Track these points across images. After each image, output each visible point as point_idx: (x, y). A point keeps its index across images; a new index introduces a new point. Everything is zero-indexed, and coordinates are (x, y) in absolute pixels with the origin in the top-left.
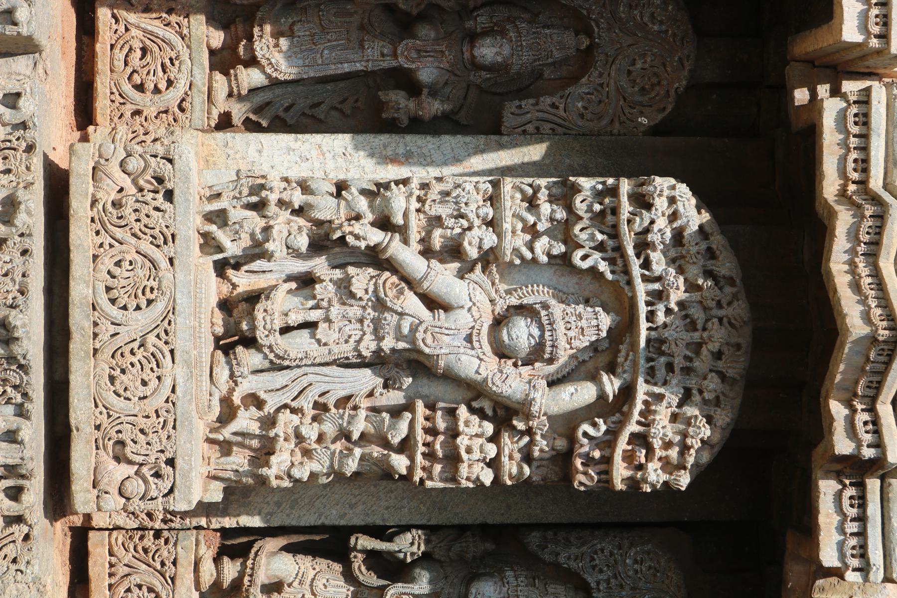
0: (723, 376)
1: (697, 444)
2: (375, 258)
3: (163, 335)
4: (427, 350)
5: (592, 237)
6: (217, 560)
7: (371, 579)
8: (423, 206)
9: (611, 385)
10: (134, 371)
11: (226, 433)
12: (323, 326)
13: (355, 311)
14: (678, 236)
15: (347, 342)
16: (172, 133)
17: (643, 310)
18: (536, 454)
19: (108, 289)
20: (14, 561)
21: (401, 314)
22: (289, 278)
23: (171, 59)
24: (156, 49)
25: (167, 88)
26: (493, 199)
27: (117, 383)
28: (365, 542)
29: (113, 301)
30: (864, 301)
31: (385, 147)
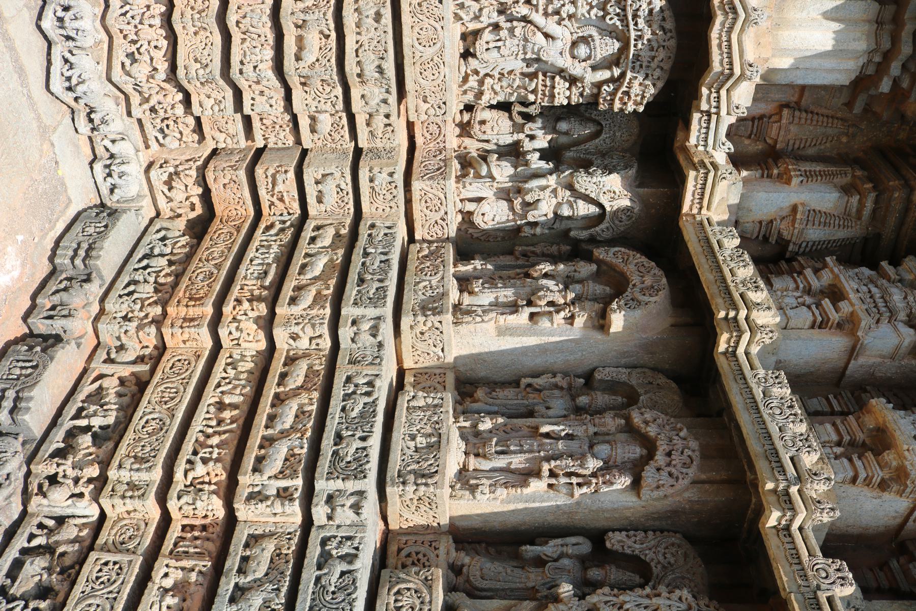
0: (662, 69)
1: (647, 95)
2: (525, 19)
5: (615, 10)
6: (461, 112)
9: (617, 72)
11: (465, 88)
12: (503, 48)
13: (516, 41)
14: (651, 11)
17: (633, 42)
18: (585, 94)
22: (489, 25)
28: (518, 108)
30: (721, 54)
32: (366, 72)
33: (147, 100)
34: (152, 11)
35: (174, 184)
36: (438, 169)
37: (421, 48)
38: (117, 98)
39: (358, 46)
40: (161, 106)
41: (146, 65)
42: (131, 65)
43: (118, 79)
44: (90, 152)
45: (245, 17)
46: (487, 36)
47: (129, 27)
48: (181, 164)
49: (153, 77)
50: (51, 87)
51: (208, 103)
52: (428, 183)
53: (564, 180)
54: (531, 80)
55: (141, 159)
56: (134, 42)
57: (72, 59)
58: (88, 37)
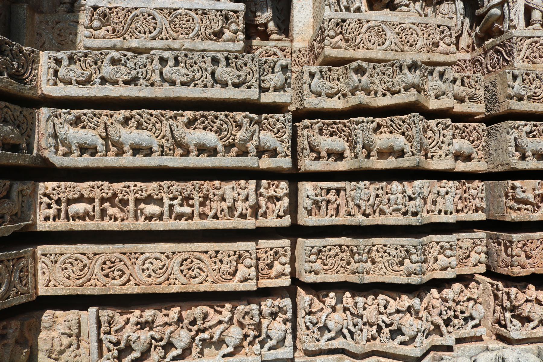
10: (408, 37)
16: (295, 51)
19: (379, 45)
20: (476, 82)
23: (266, 53)
25: (277, 55)
27: (413, 44)
29: (383, 44)
32: (416, 81)
33: (437, 327)
35: (525, 314)
36: (498, 52)
37: (387, 43)
39: (388, 94)
40: (444, 313)
41: (404, 319)
42: (403, 334)
43: (418, 349)
45: (359, 206)
48: (501, 305)
49: (417, 312)
51: (443, 260)
52: (515, 54)
56: (379, 328)
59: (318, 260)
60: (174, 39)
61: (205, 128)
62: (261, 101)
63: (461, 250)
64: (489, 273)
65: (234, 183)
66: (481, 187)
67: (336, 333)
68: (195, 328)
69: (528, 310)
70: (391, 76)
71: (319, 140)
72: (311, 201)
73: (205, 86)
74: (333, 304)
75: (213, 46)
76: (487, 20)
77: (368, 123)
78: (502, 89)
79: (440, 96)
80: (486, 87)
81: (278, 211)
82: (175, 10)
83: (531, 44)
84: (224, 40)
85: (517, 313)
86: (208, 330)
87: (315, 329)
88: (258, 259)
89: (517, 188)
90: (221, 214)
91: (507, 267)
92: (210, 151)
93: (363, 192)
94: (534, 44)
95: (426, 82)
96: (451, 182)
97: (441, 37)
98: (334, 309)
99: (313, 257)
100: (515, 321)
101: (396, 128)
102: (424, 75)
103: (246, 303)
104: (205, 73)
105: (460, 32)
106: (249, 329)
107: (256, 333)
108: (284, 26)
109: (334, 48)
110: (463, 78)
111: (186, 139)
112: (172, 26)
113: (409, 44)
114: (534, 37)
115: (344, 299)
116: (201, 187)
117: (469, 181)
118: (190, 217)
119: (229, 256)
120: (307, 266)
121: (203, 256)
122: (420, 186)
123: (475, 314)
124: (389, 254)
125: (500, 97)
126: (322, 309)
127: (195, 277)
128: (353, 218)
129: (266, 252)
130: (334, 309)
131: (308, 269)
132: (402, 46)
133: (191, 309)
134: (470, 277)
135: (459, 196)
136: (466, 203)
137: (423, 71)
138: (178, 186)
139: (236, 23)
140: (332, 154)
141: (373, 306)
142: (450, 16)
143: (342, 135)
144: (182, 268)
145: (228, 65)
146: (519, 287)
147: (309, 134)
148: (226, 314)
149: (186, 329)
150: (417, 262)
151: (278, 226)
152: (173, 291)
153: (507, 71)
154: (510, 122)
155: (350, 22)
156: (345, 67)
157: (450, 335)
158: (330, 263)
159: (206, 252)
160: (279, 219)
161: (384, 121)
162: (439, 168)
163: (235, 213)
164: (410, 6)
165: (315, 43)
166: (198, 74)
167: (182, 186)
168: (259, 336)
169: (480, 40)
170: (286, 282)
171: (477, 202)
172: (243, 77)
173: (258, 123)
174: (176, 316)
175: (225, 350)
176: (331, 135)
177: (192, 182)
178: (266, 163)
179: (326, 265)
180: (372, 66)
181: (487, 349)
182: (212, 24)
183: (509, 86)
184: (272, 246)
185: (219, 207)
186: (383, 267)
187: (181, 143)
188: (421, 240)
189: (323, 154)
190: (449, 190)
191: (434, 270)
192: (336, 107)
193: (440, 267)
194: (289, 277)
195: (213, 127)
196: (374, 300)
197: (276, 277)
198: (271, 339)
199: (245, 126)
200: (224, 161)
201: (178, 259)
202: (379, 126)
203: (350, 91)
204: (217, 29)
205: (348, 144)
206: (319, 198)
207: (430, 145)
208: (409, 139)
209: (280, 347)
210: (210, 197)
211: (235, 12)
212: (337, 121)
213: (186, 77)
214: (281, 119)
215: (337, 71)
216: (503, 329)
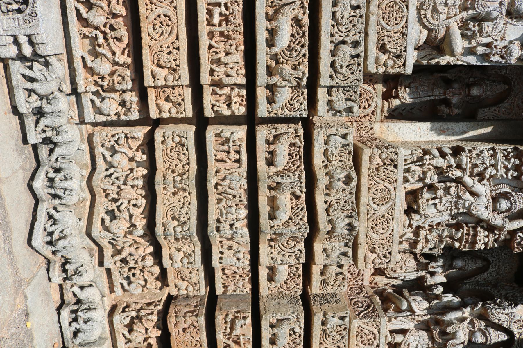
2: (459, 181)
3: (390, 213)
4: (474, 213)
7: (423, 260)
8: (471, 160)
10: (380, 225)
12: (438, 204)
13: (450, 199)
15: (447, 210)
16: (372, 124)
19: (373, 199)
20: (339, 286)
21: (465, 200)
24: (365, 94)
26: (494, 156)
27: (374, 229)
29: (374, 203)
31: (441, 126)
32: (338, 230)
33: (119, 252)
34: (135, 174)
35: (135, 327)
36: (368, 306)
37: (375, 206)
38: (91, 250)
39: (327, 206)
40: (132, 258)
41: (124, 222)
42: (111, 221)
43: (98, 234)
44: (57, 297)
45: (224, 179)
46: (427, 195)
47: (113, 187)
48: (142, 309)
49: (131, 233)
50: (33, 242)
52: (365, 321)
53: (477, 312)
54: (457, 230)
55: (106, 304)
56: (115, 201)
57: (56, 215)
58: (74, 196)
59: (175, 144)
60: (379, 6)
61: (293, 35)
62: (319, 88)
63: (189, 272)
64: (170, 298)
65: (242, 63)
66: (245, 290)
67: (110, 162)
68: (108, 30)
69: (138, 329)
70: (343, 208)
71: (285, 143)
72: (228, 136)
73: (332, 35)
74: (136, 158)
75: (372, 44)
76: (398, 298)
77: (300, 189)
78: (332, 308)
79: (326, 253)
80: (336, 295)
81: (218, 105)
82: (407, 6)
83: (373, 334)
84: (377, 54)
85: (135, 321)
86: (106, 42)
87: (112, 143)
88: (173, 87)
89: (245, 320)
90: (213, 52)
91: (176, 313)
92: (271, 40)
93: (237, 183)
94: (374, 336)
95: (338, 240)
96: (248, 263)
97: (381, 255)
98: (131, 160)
99: (177, 139)
100: (128, 320)
101: (296, 212)
102: (344, 238)
103: (133, 77)
104: (344, 35)
105: (389, 276)
106: (109, 81)
107: (106, 87)
108: (397, 115)
109: (371, 157)
110: (343, 274)
111: (282, 17)
112: (391, 4)
113: (374, 226)
114: (380, 336)
115: (141, 168)
116: (238, 33)
117: (250, 280)
118: (210, 23)
119: (175, 60)
120: (169, 134)
121: (173, 36)
122: (243, 234)
123: (133, 286)
124: (182, 208)
125: (325, 307)
126: (131, 149)
127: (154, 29)
128: (213, 175)
129: (180, 95)
130: (131, 160)
131: (166, 135)
132: (372, 219)
133: (125, 25)
134: (166, 283)
135: (237, 271)
136: (231, 277)
137: (348, 237)
138: (238, 11)
139: (394, 65)
140: (272, 155)
141: (135, 195)
142: (403, 267)
143: (290, 164)
144: (162, 16)
145: (353, 57)
146: (158, 323)
147: (290, 134)
148: (122, 59)
149: (106, 21)
150: (175, 232)
151: (204, 105)
152: (140, 8)
153: (349, 312)
154: (303, 314)
155: (394, 172)
156: (352, 167)
157: (113, 263)
158: (172, 154)
159: (177, 39)
160: (211, 106)
161: (302, 202)
162: (261, 252)
163: (215, 65)
164: (410, 228)
165: (377, 142)
166: (343, 28)
167: (238, 14)
168: (104, 91)
169: (381, 293)
170: (154, 114)
171: (231, 287)
172: (340, 71)
173: (299, 85)
174: (117, 12)
175: (89, 59)
176: (290, 155)
177: (242, 24)
178: (262, 94)
179: (171, 151)
180: (352, 191)
181: (103, 296)
182: (393, 43)
183: (334, 313)
184: (186, 100)
185: (219, 50)
186: (170, 202)
187: (278, 13)
188: (195, 234)
189: (272, 147)
190: (241, 261)
191: (170, 248)
192: (315, 159)
193: (172, 254)
194: (158, 117)
195: (294, 43)
196: (141, 195)
197: (157, 105)
198: (101, 102)
199: (295, 73)
200: (262, 54)
201: (170, 12)
202: (298, 198)
203: (330, 171)
204: (388, 47)
205: (282, 170)
206: (231, 144)
207: (282, 244)
208: (286, 224)
209: (94, 110)
210: (229, 41)
211: (404, 65)
212: (302, 160)
213: (340, 17)
214: (303, 107)
215: (349, 160)
216: (121, 310)
